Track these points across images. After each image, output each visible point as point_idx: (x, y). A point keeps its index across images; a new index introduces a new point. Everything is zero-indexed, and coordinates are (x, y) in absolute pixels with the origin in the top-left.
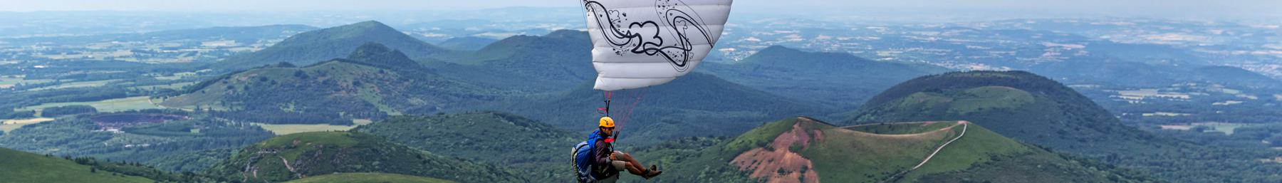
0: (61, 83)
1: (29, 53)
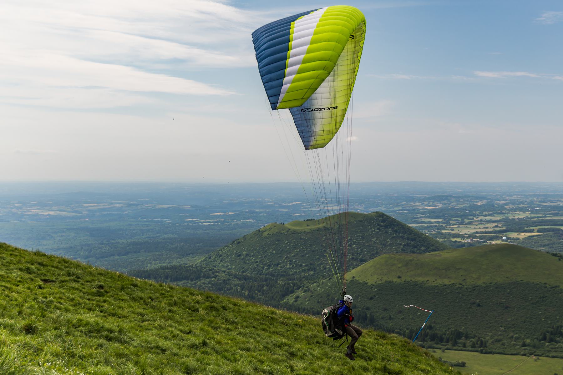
0: (547, 217)
1: (533, 202)
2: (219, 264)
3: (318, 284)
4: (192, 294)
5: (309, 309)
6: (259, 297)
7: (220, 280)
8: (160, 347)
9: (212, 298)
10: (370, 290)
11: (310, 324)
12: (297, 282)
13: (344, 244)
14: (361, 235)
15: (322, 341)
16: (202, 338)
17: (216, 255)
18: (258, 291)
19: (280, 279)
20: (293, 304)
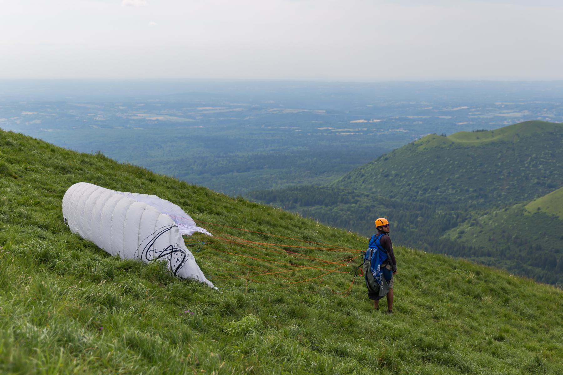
2: (361, 185)
5: (477, 248)
7: (362, 207)
12: (462, 212)
14: (550, 152)
17: (357, 174)
19: (440, 208)
20: (455, 240)
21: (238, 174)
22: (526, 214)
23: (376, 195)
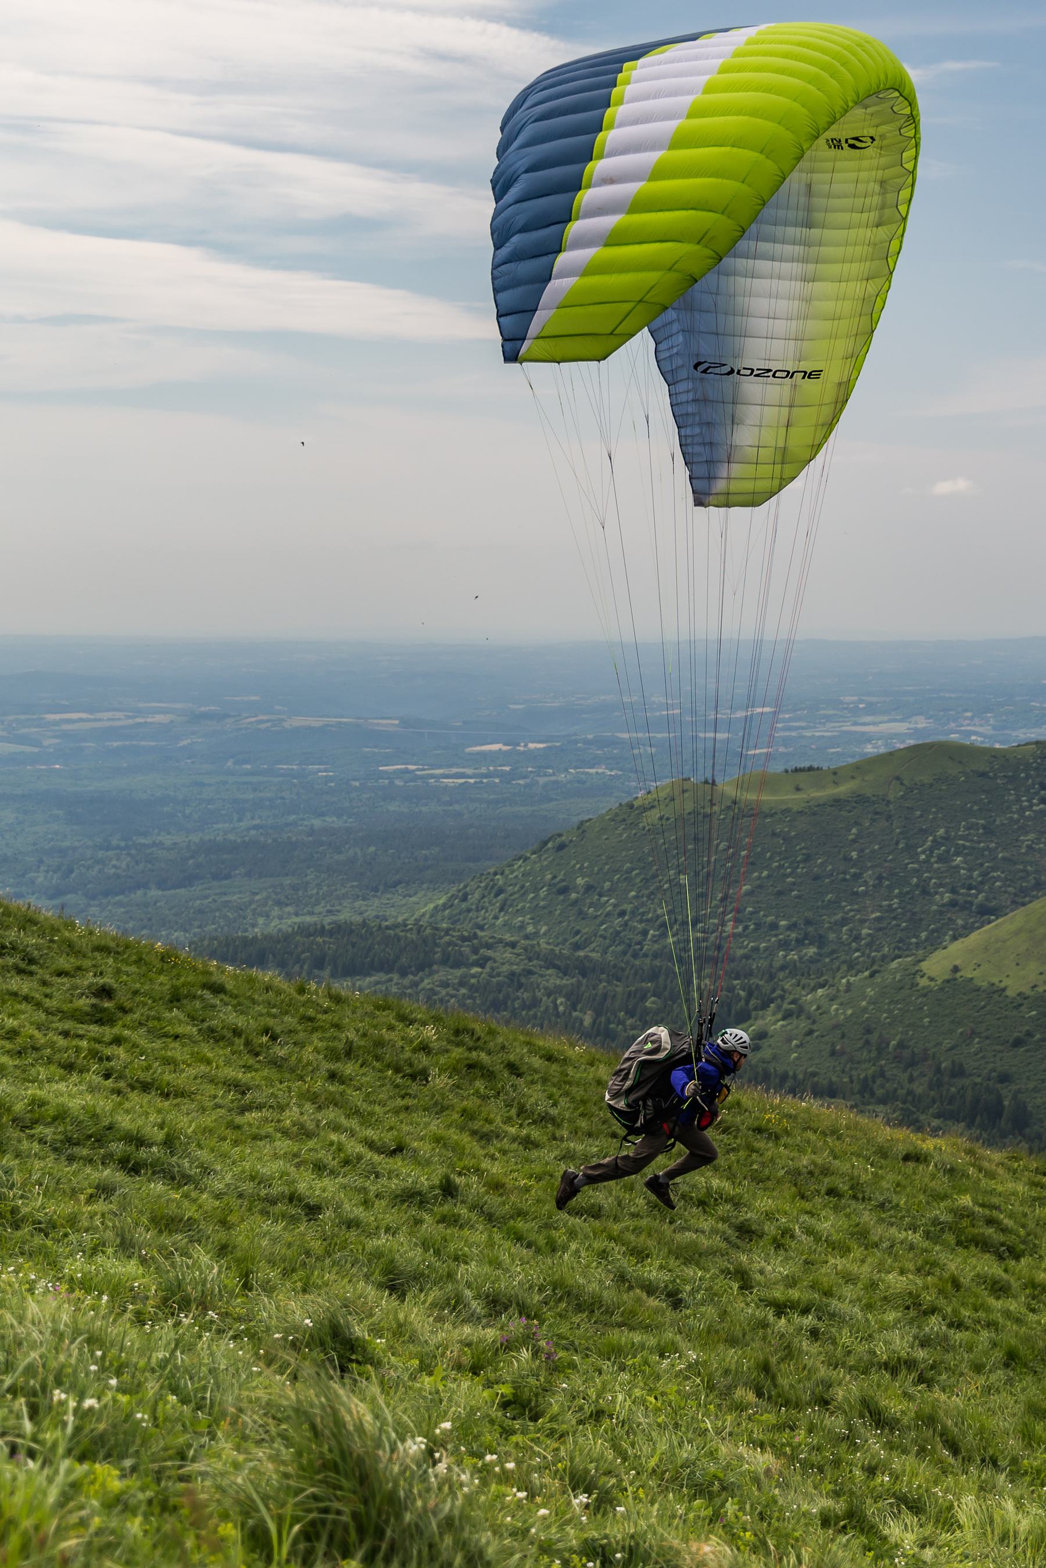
2: (496, 918)
3: (832, 991)
4: (406, 1020)
5: (801, 1077)
6: (632, 1032)
7: (499, 975)
8: (300, 1200)
9: (472, 1033)
10: (1015, 1013)
11: (805, 1129)
12: (761, 983)
13: (923, 852)
14: (982, 822)
15: (846, 1188)
16: (441, 1171)
17: (486, 888)
18: (626, 1014)
21: (160, 893)
22: (923, 982)
23: (535, 942)
